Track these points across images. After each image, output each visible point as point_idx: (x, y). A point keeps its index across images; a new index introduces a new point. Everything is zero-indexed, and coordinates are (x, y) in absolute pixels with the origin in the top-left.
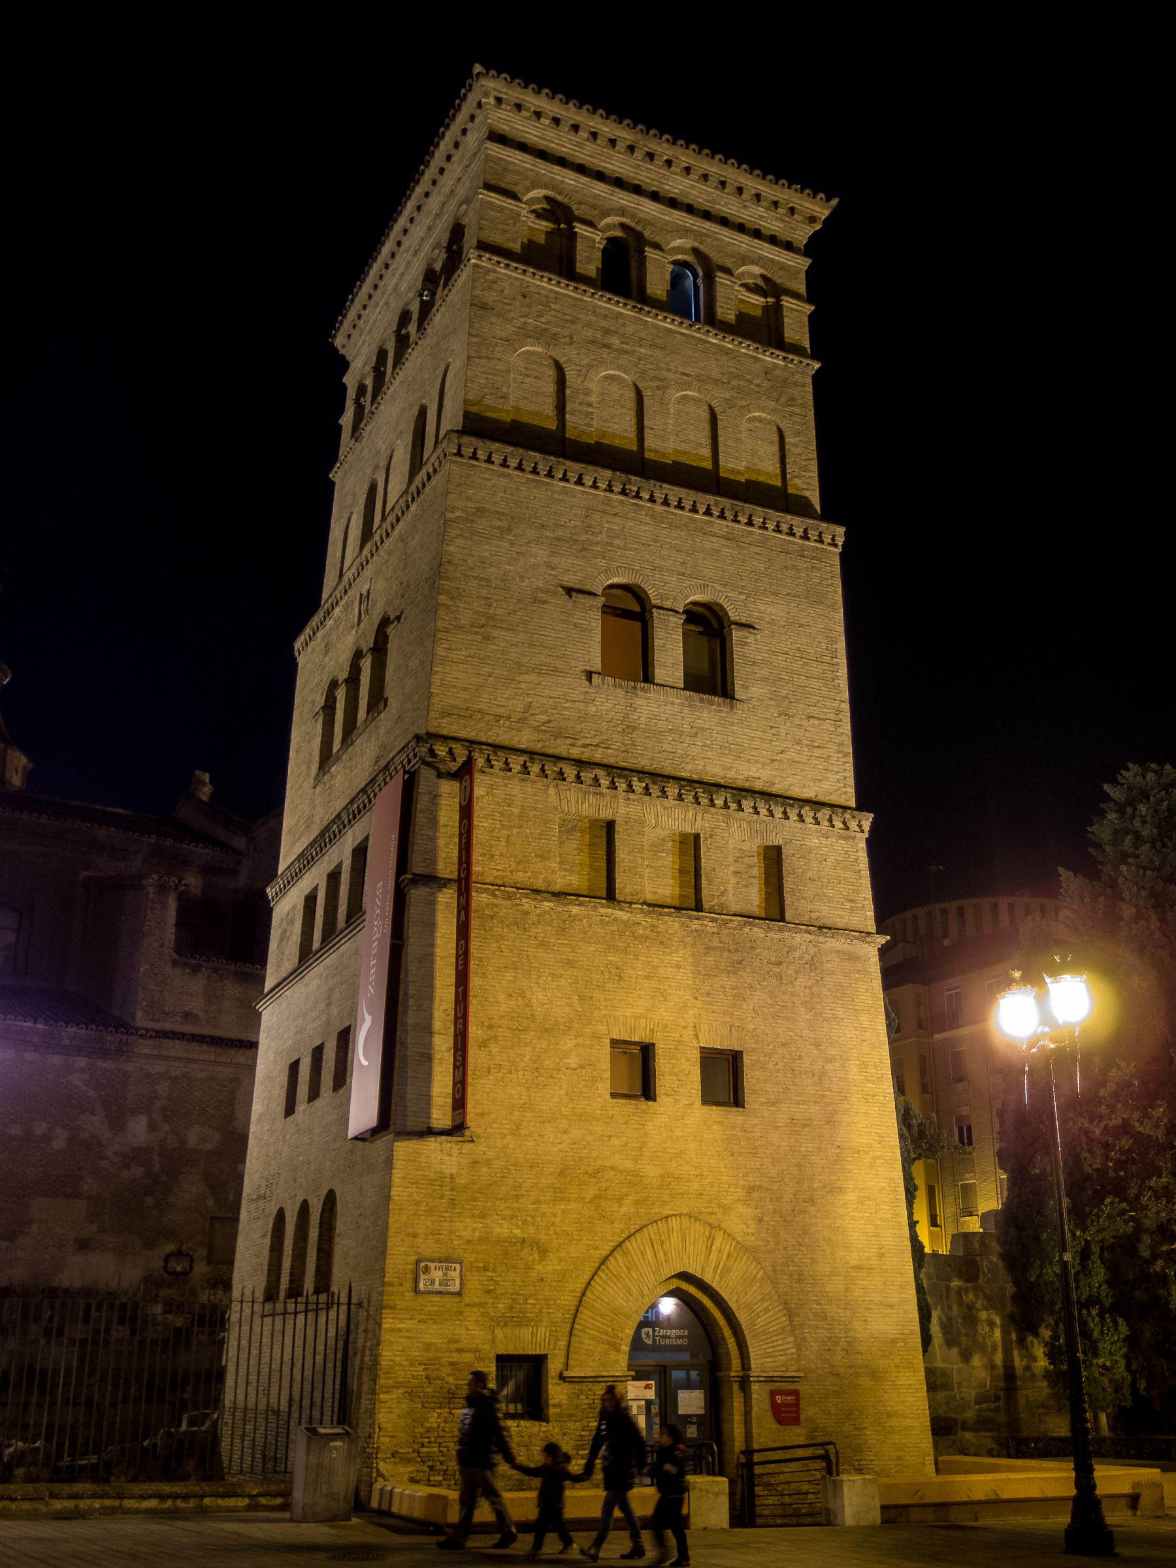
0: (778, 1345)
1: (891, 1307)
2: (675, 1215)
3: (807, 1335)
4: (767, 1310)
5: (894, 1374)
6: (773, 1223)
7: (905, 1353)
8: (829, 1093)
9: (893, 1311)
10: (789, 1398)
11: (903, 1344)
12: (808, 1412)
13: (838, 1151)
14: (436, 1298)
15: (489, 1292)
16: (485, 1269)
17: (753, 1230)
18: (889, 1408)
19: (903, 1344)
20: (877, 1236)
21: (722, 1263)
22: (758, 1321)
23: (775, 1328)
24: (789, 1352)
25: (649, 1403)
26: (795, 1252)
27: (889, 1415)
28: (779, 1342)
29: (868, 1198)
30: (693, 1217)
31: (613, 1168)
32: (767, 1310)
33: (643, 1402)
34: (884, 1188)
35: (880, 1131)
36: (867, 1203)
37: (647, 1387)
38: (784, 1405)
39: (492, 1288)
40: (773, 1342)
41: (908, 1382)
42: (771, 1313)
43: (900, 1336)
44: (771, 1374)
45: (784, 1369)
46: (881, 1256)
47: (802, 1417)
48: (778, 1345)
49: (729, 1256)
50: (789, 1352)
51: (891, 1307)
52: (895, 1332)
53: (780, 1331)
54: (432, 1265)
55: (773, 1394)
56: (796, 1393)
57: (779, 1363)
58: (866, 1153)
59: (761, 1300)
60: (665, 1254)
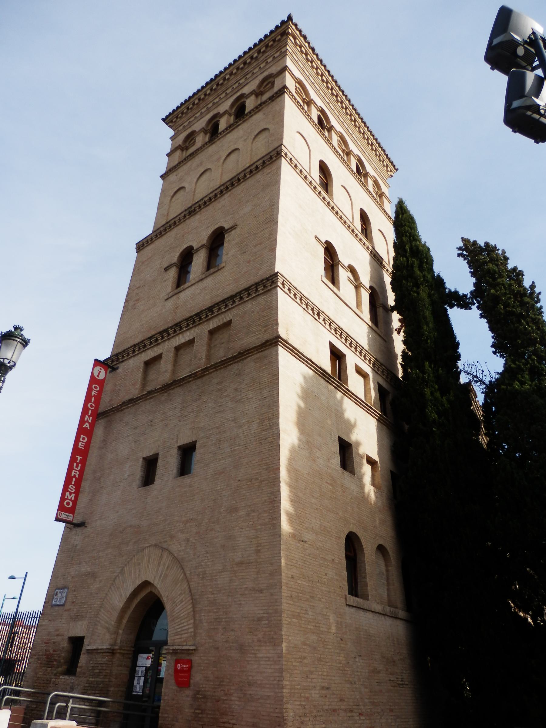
0: (184, 626)
1: (261, 591)
2: (148, 547)
3: (203, 617)
4: (182, 601)
5: (256, 648)
6: (194, 541)
7: (268, 629)
8: (238, 448)
9: (261, 595)
10: (185, 666)
11: (266, 622)
12: (197, 677)
13: (239, 483)
14: (57, 608)
15: (73, 602)
16: (75, 591)
17: (183, 548)
18: (250, 678)
19: (266, 622)
20: (257, 537)
21: (164, 572)
22: (176, 609)
23: (184, 614)
24: (190, 631)
25: (147, 669)
26: (204, 559)
27: (250, 684)
28: (185, 624)
29: (254, 511)
30: (156, 546)
31: (131, 526)
32: (182, 601)
33: (144, 668)
34: (265, 501)
35: (267, 461)
36: (252, 514)
37: (148, 658)
38: (182, 671)
39: (74, 600)
40: (181, 624)
41: (269, 655)
42: (183, 603)
43: (265, 615)
44: (177, 647)
45: (185, 643)
46: (258, 551)
47: (192, 681)
48: (184, 626)
49: (168, 567)
50: (190, 631)
51: (261, 591)
52: (262, 612)
53: (186, 616)
54: (59, 591)
55: (177, 662)
56: (190, 662)
57: (183, 640)
58: (257, 479)
59: (180, 595)
60: (139, 571)
